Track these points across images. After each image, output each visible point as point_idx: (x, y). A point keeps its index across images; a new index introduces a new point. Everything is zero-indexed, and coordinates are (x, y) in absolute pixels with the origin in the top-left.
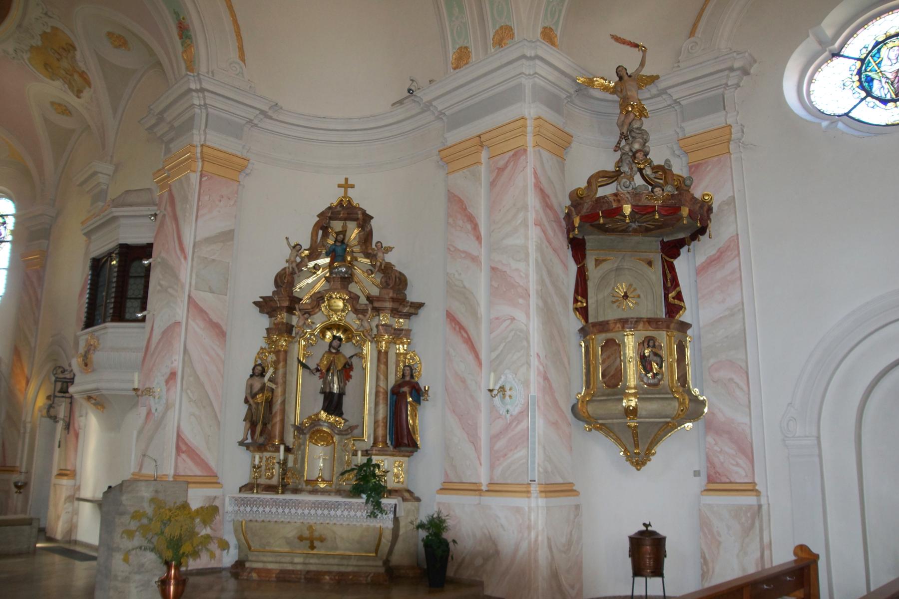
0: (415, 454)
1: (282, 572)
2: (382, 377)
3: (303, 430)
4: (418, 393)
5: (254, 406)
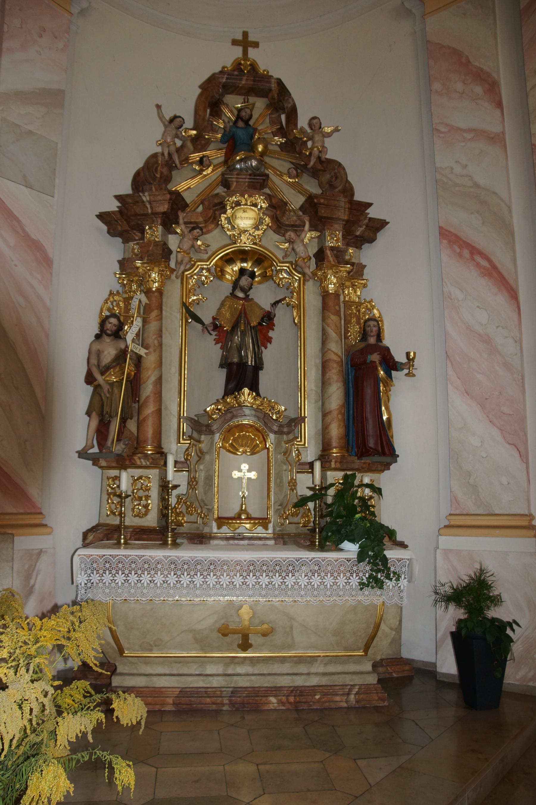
0: (393, 467)
1: (184, 692)
2: (332, 334)
3: (208, 426)
4: (391, 365)
5: (106, 387)
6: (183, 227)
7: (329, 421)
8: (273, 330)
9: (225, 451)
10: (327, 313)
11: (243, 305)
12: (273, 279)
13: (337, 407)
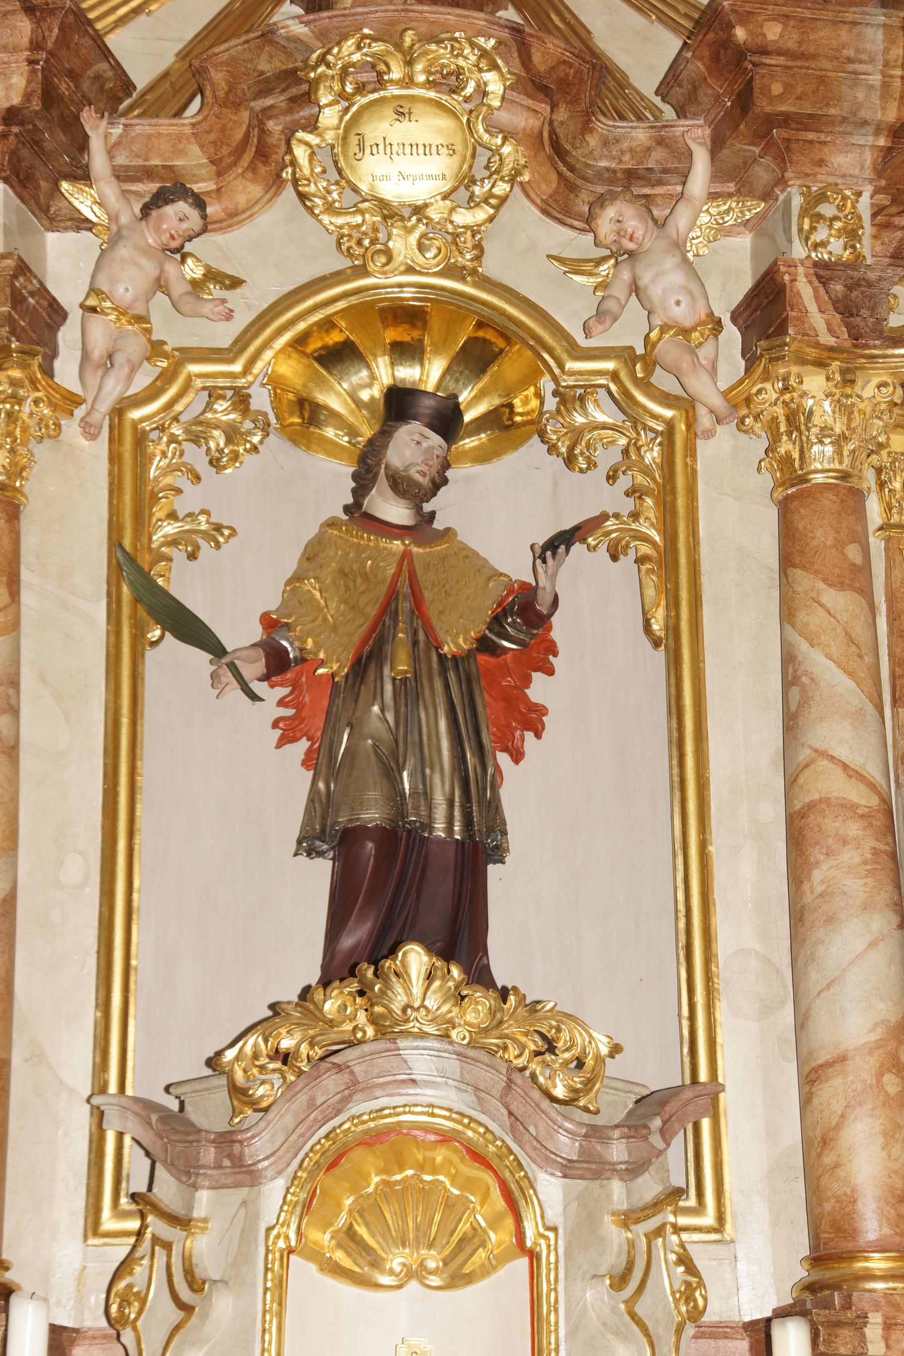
3: (227, 1141)
6: (110, 190)
7: (838, 1107)
8: (550, 672)
9: (313, 1267)
10: (803, 580)
11: (406, 555)
12: (542, 434)
13: (873, 1037)
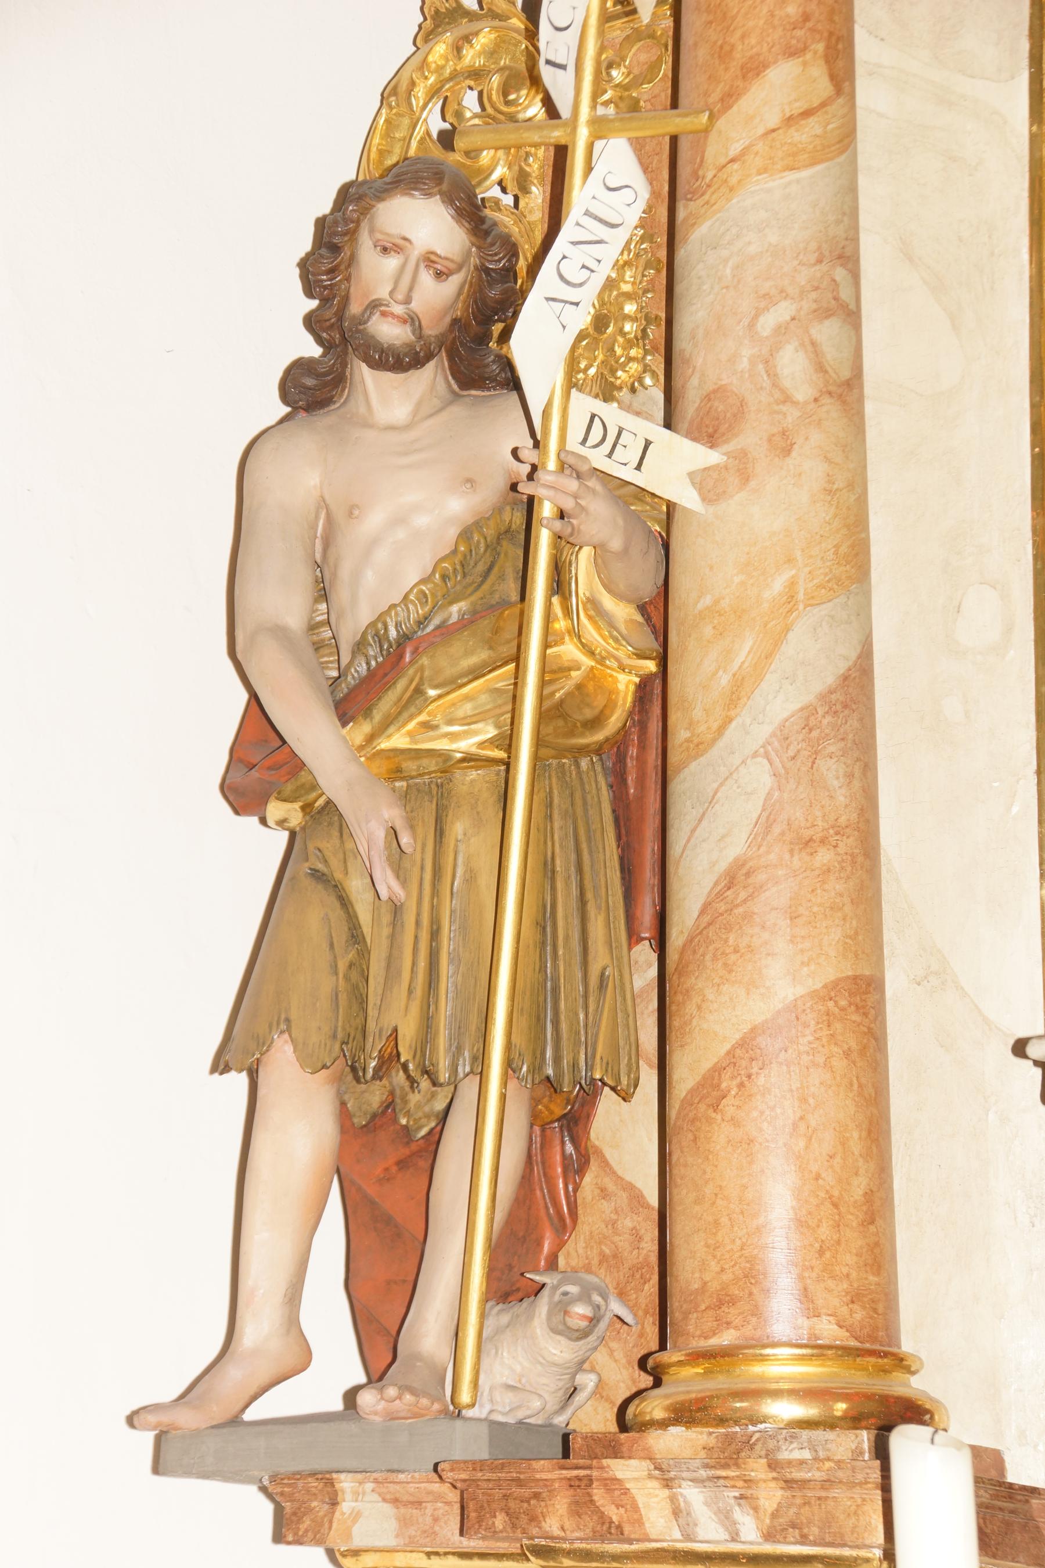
5: (373, 817)
